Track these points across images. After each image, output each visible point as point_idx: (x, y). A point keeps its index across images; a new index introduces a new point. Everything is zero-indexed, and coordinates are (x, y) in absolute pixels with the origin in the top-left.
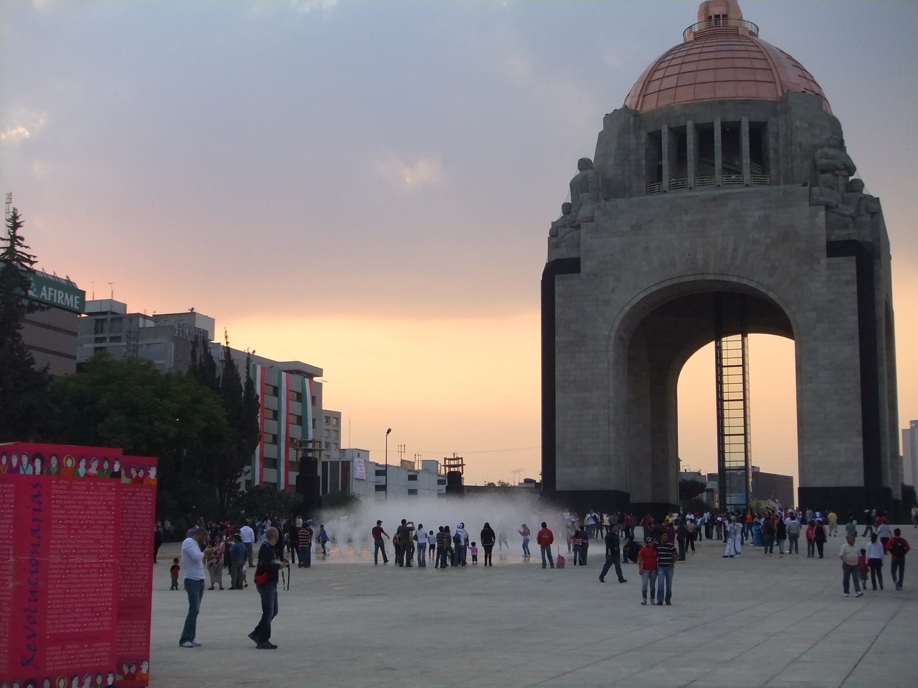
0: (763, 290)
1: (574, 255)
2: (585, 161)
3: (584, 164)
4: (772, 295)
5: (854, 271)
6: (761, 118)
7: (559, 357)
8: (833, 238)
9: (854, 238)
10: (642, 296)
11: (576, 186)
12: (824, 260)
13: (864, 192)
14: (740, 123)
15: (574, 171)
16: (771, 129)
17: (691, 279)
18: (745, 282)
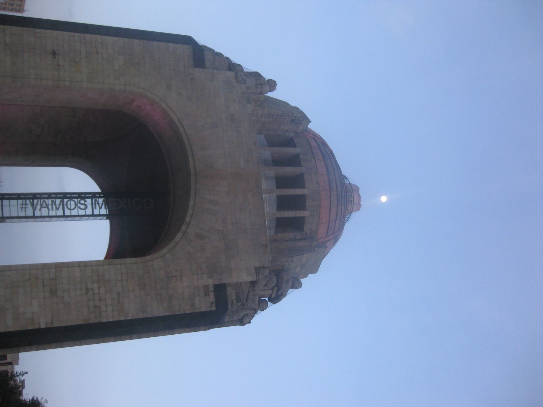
0: (184, 227)
1: (207, 63)
2: (275, 85)
3: (272, 85)
4: (179, 235)
5: (203, 310)
6: (307, 228)
7: (120, 41)
8: (229, 289)
9: (230, 306)
10: (175, 119)
11: (257, 75)
12: (210, 282)
13: (259, 311)
14: (304, 209)
15: (267, 76)
16: (298, 236)
17: (191, 164)
18: (190, 212)
